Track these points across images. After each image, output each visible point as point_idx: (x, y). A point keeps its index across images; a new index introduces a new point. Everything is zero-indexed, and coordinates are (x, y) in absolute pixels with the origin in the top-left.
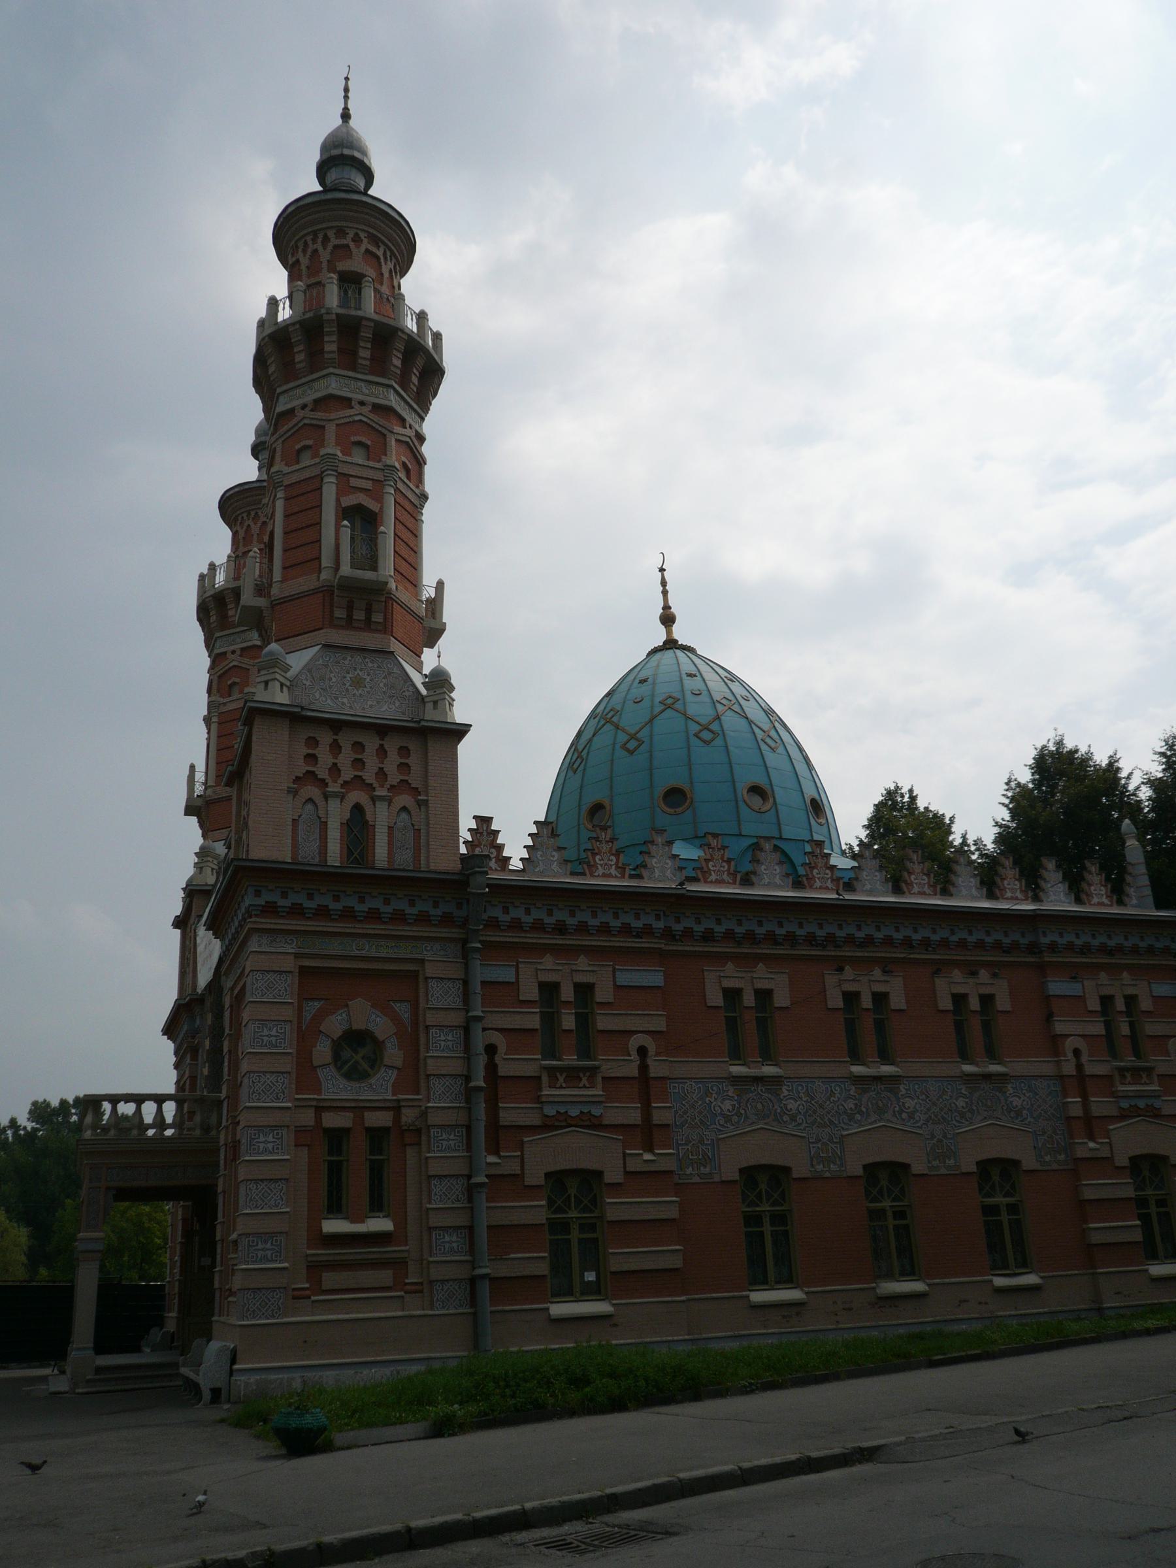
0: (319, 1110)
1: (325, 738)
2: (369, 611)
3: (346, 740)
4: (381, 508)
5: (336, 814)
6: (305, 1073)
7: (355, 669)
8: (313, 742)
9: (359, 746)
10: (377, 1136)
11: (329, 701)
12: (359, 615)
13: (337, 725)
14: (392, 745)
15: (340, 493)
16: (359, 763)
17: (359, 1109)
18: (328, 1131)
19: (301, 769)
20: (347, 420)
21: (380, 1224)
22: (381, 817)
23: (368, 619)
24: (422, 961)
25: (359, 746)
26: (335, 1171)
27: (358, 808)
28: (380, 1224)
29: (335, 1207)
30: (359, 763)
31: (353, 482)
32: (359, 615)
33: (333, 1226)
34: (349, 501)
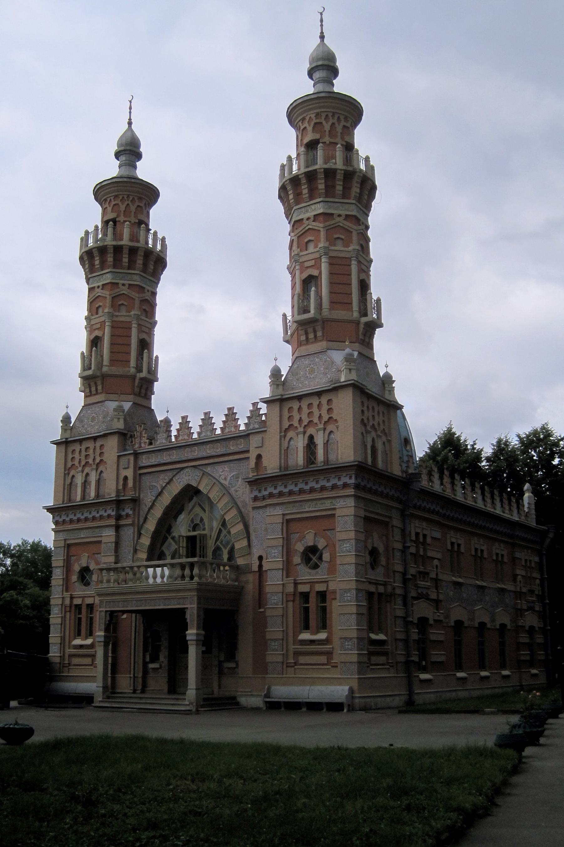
0: (296, 584)
1: (295, 405)
2: (315, 332)
3: (304, 404)
4: (320, 273)
5: (300, 443)
6: (288, 568)
7: (310, 365)
9: (310, 405)
10: (322, 596)
11: (300, 385)
12: (311, 336)
13: (300, 398)
14: (324, 400)
15: (301, 272)
16: (310, 414)
17: (312, 583)
18: (301, 593)
19: (286, 425)
20: (304, 231)
21: (322, 636)
22: (320, 440)
23: (315, 337)
24: (335, 509)
25: (310, 405)
26: (306, 610)
27: (311, 438)
28: (322, 636)
29: (306, 627)
30: (310, 414)
31: (307, 264)
32: (311, 336)
33: (305, 636)
34: (305, 275)
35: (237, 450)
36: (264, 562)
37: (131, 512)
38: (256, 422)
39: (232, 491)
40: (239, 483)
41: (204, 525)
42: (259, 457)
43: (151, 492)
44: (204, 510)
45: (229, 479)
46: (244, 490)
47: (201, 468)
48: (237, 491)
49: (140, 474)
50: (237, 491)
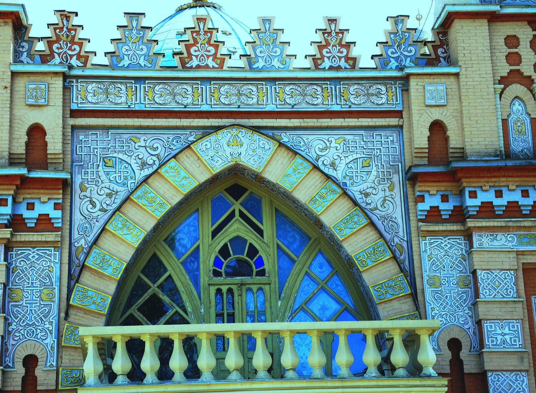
8: (512, 41)
35: (369, 107)
36: (464, 354)
37: (56, 214)
38: (406, 57)
39: (355, 191)
40: (372, 177)
41: (260, 262)
42: (437, 127)
43: (107, 174)
44: (261, 232)
45: (341, 166)
46: (388, 193)
47: (270, 133)
48: (367, 195)
49: (74, 128)
50: (367, 195)
